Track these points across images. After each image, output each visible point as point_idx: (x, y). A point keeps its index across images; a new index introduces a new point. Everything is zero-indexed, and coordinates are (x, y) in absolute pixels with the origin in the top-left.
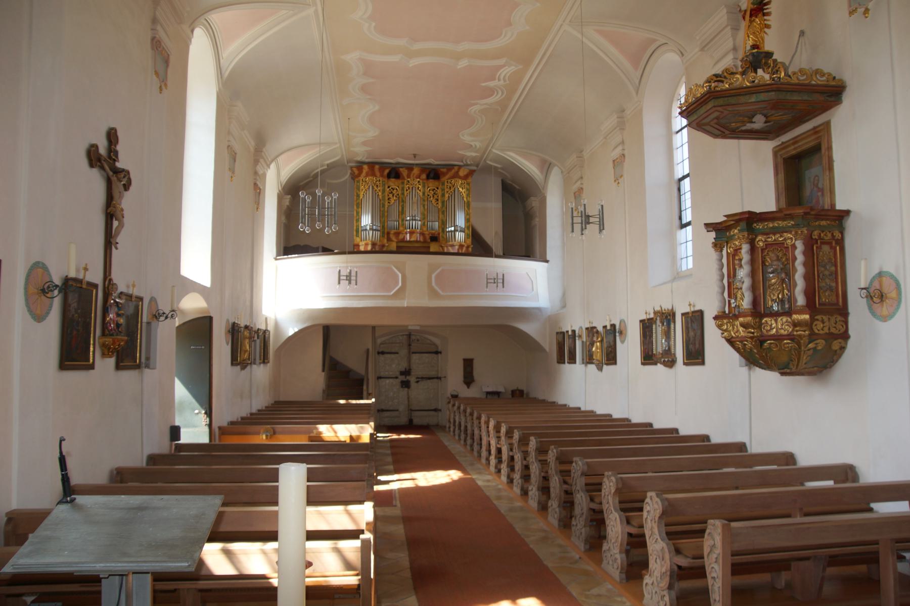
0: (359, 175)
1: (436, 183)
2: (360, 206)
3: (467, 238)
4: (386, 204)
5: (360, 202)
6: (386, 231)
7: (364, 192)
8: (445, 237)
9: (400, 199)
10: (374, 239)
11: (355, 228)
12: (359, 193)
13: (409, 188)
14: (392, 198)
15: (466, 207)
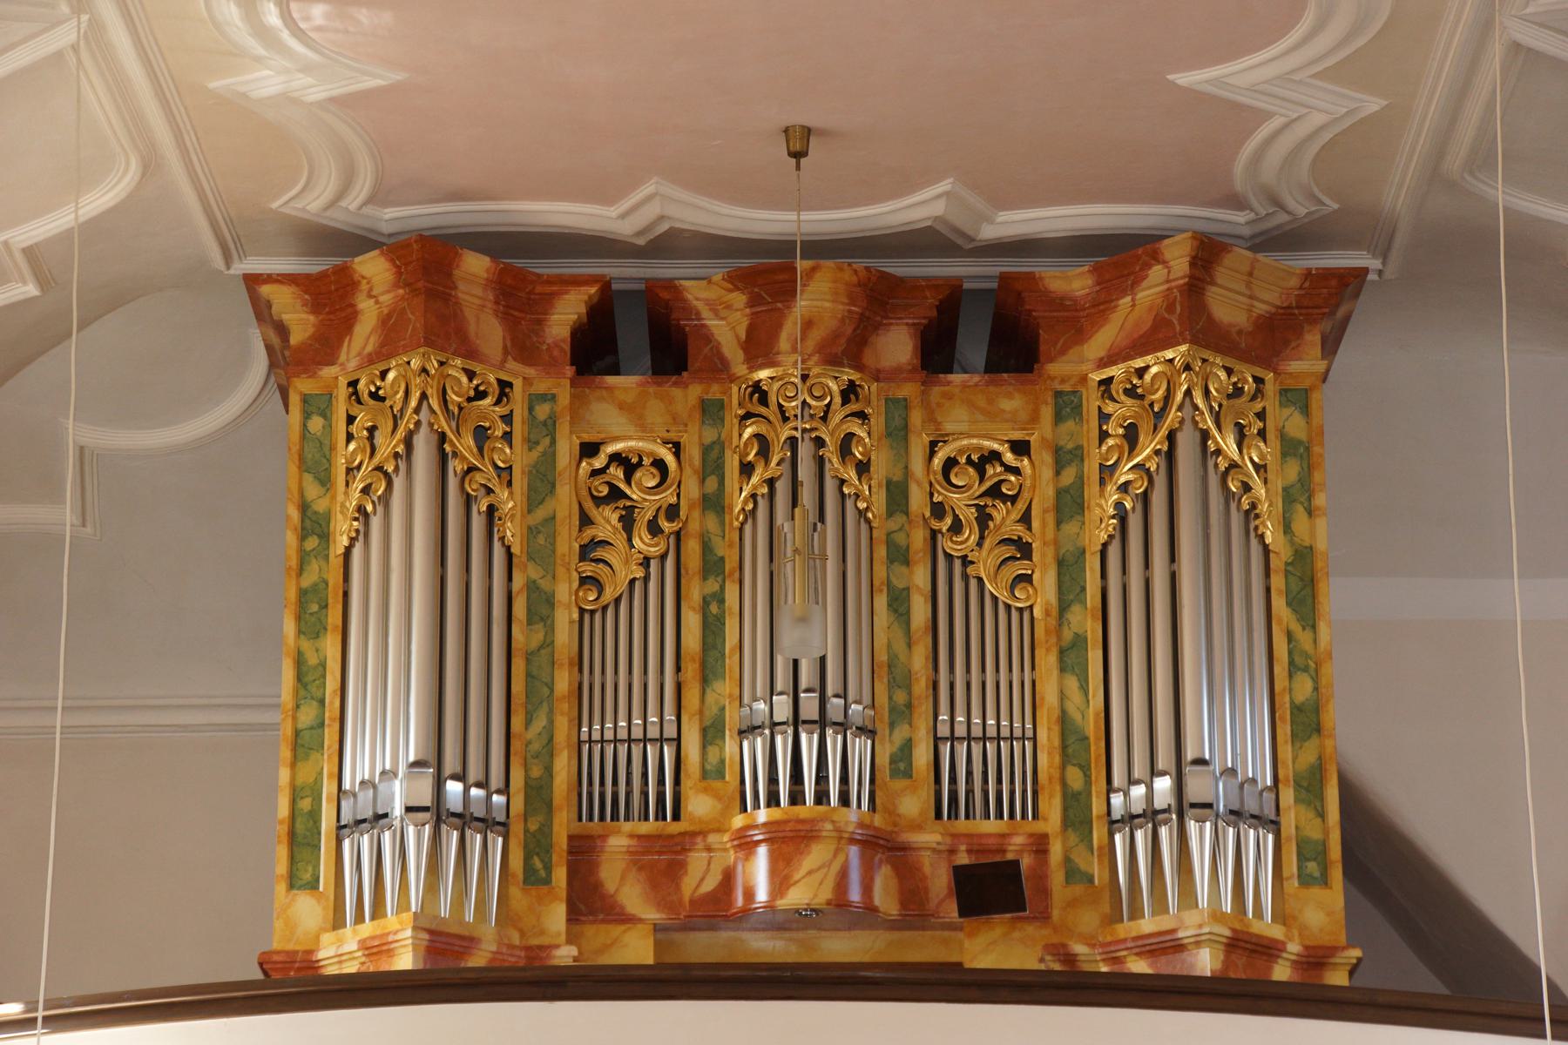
0: (325, 348)
1: (1012, 401)
2: (334, 616)
3: (1305, 880)
4: (564, 590)
5: (334, 578)
6: (562, 826)
7: (366, 491)
8: (1098, 872)
9: (692, 547)
10: (444, 911)
11: (283, 810)
12: (320, 506)
13: (764, 453)
14: (619, 540)
15: (1279, 603)
